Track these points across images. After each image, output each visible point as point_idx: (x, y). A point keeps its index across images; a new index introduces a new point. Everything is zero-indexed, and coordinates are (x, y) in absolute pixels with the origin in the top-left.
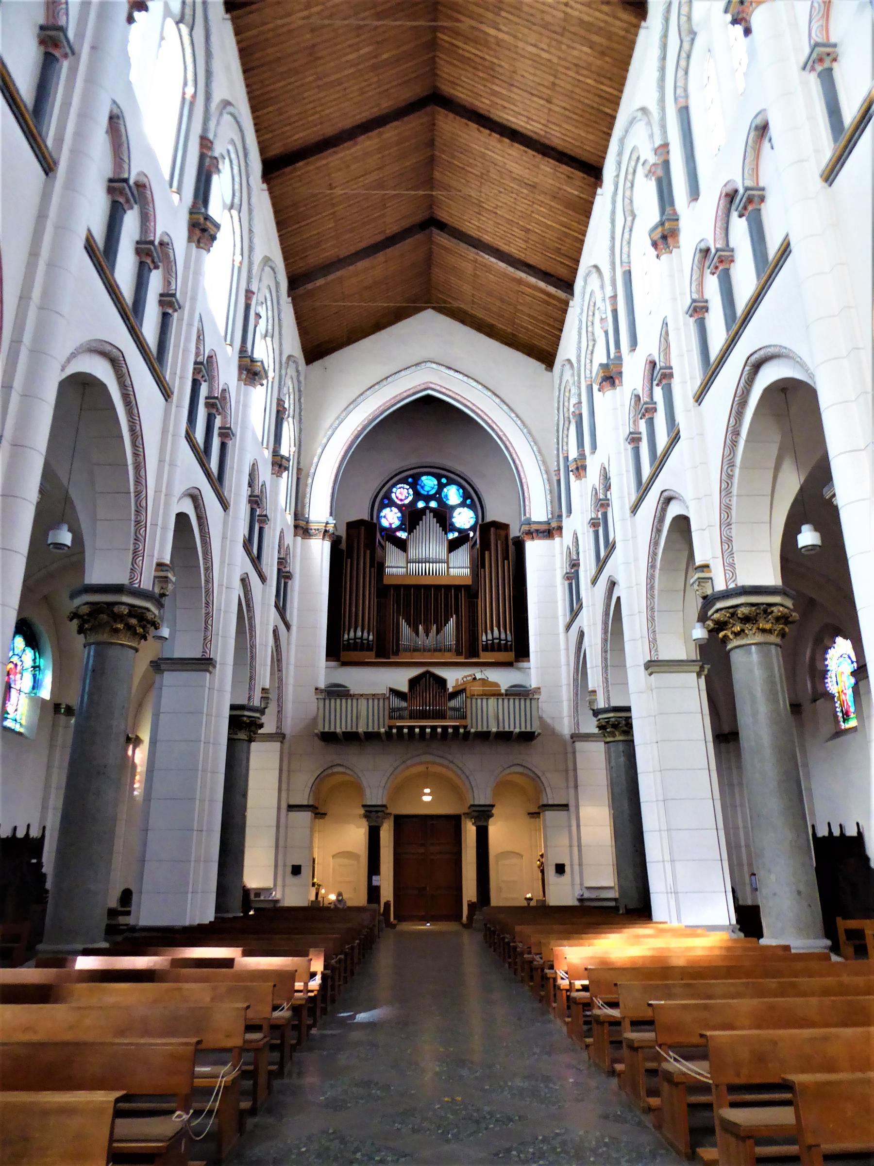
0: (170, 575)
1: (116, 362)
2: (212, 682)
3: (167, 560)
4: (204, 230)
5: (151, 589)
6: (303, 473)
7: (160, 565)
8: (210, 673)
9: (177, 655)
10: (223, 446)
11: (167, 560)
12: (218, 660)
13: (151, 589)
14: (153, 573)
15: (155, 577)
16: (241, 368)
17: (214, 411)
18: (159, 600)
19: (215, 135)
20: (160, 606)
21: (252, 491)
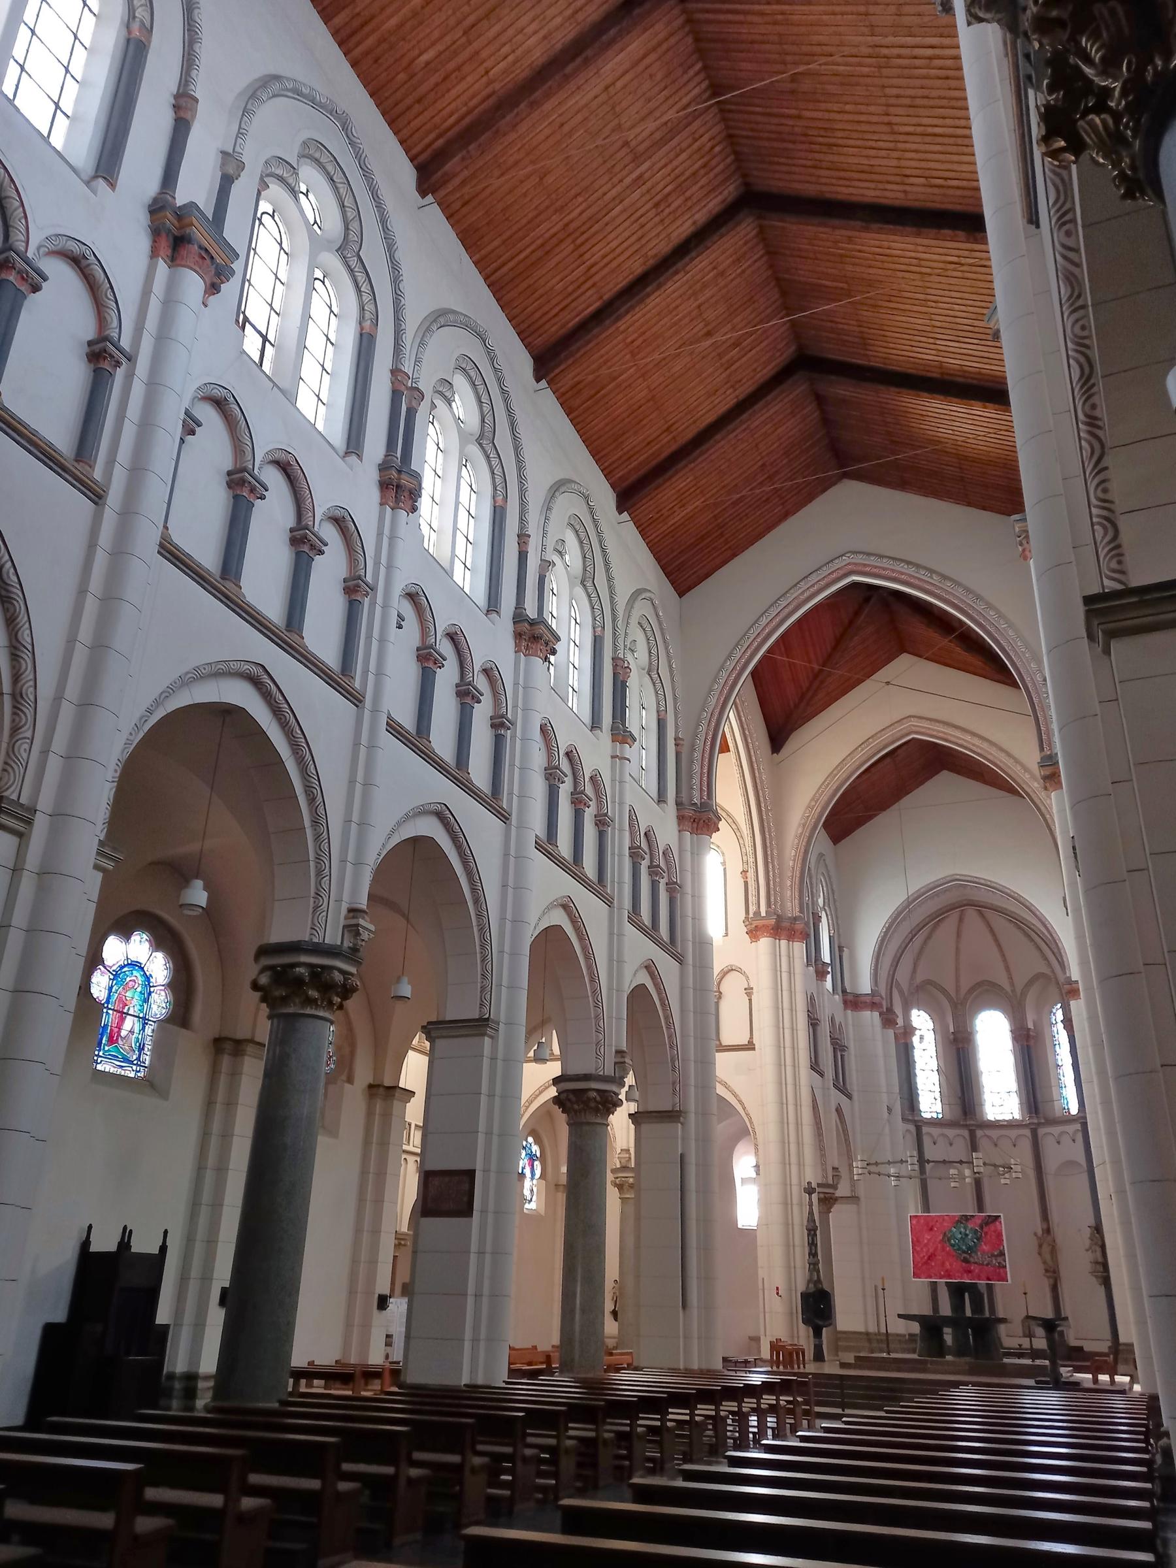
0: (361, 922)
1: (259, 680)
2: (494, 1048)
3: (363, 902)
4: (398, 486)
5: (339, 943)
6: (686, 744)
7: (353, 911)
8: (491, 1037)
9: (449, 1017)
10: (498, 743)
11: (363, 902)
12: (502, 1018)
13: (339, 943)
14: (342, 922)
15: (344, 927)
16: (518, 635)
17: (468, 700)
18: (353, 955)
19: (418, 361)
20: (357, 963)
21: (575, 789)
